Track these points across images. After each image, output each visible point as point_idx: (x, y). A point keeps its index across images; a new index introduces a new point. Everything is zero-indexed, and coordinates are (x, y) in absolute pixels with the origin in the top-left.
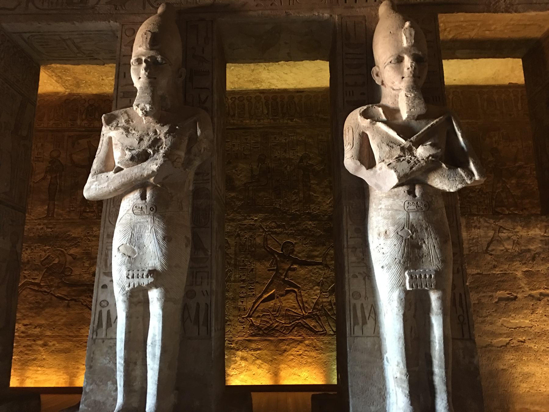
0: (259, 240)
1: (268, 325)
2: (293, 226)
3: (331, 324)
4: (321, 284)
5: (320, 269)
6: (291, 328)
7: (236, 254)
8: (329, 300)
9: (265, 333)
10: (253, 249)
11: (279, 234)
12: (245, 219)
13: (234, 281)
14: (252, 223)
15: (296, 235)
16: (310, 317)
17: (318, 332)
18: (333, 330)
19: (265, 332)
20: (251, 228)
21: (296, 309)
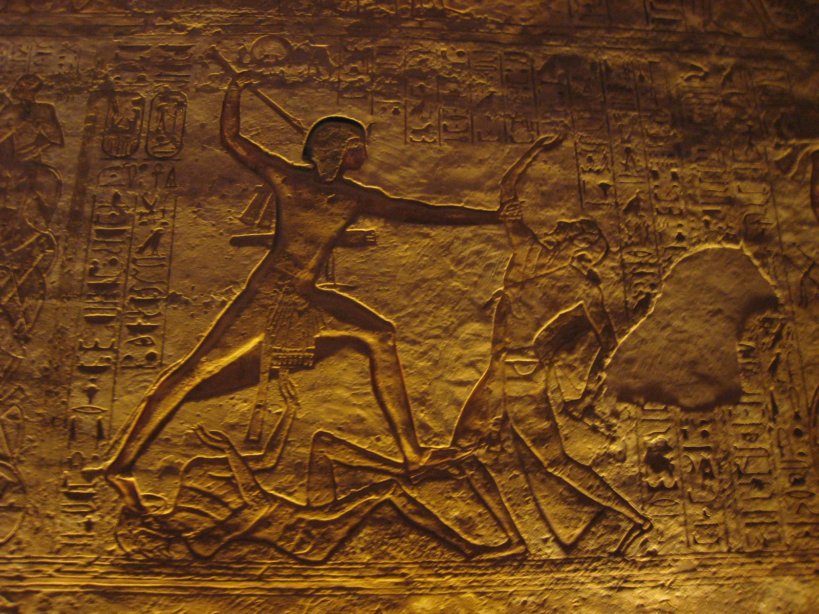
0: (200, 113)
1: (219, 515)
2: (366, 56)
3: (548, 511)
4: (498, 313)
5: (488, 240)
6: (340, 533)
7: (83, 170)
8: (538, 387)
9: (197, 557)
10: (170, 148)
11: (295, 85)
12: (144, 28)
13: (62, 293)
14: (174, 43)
15: (379, 94)
16: (444, 476)
17: (486, 549)
18: (557, 540)
19: (200, 549)
20: (169, 63)
21: (367, 434)
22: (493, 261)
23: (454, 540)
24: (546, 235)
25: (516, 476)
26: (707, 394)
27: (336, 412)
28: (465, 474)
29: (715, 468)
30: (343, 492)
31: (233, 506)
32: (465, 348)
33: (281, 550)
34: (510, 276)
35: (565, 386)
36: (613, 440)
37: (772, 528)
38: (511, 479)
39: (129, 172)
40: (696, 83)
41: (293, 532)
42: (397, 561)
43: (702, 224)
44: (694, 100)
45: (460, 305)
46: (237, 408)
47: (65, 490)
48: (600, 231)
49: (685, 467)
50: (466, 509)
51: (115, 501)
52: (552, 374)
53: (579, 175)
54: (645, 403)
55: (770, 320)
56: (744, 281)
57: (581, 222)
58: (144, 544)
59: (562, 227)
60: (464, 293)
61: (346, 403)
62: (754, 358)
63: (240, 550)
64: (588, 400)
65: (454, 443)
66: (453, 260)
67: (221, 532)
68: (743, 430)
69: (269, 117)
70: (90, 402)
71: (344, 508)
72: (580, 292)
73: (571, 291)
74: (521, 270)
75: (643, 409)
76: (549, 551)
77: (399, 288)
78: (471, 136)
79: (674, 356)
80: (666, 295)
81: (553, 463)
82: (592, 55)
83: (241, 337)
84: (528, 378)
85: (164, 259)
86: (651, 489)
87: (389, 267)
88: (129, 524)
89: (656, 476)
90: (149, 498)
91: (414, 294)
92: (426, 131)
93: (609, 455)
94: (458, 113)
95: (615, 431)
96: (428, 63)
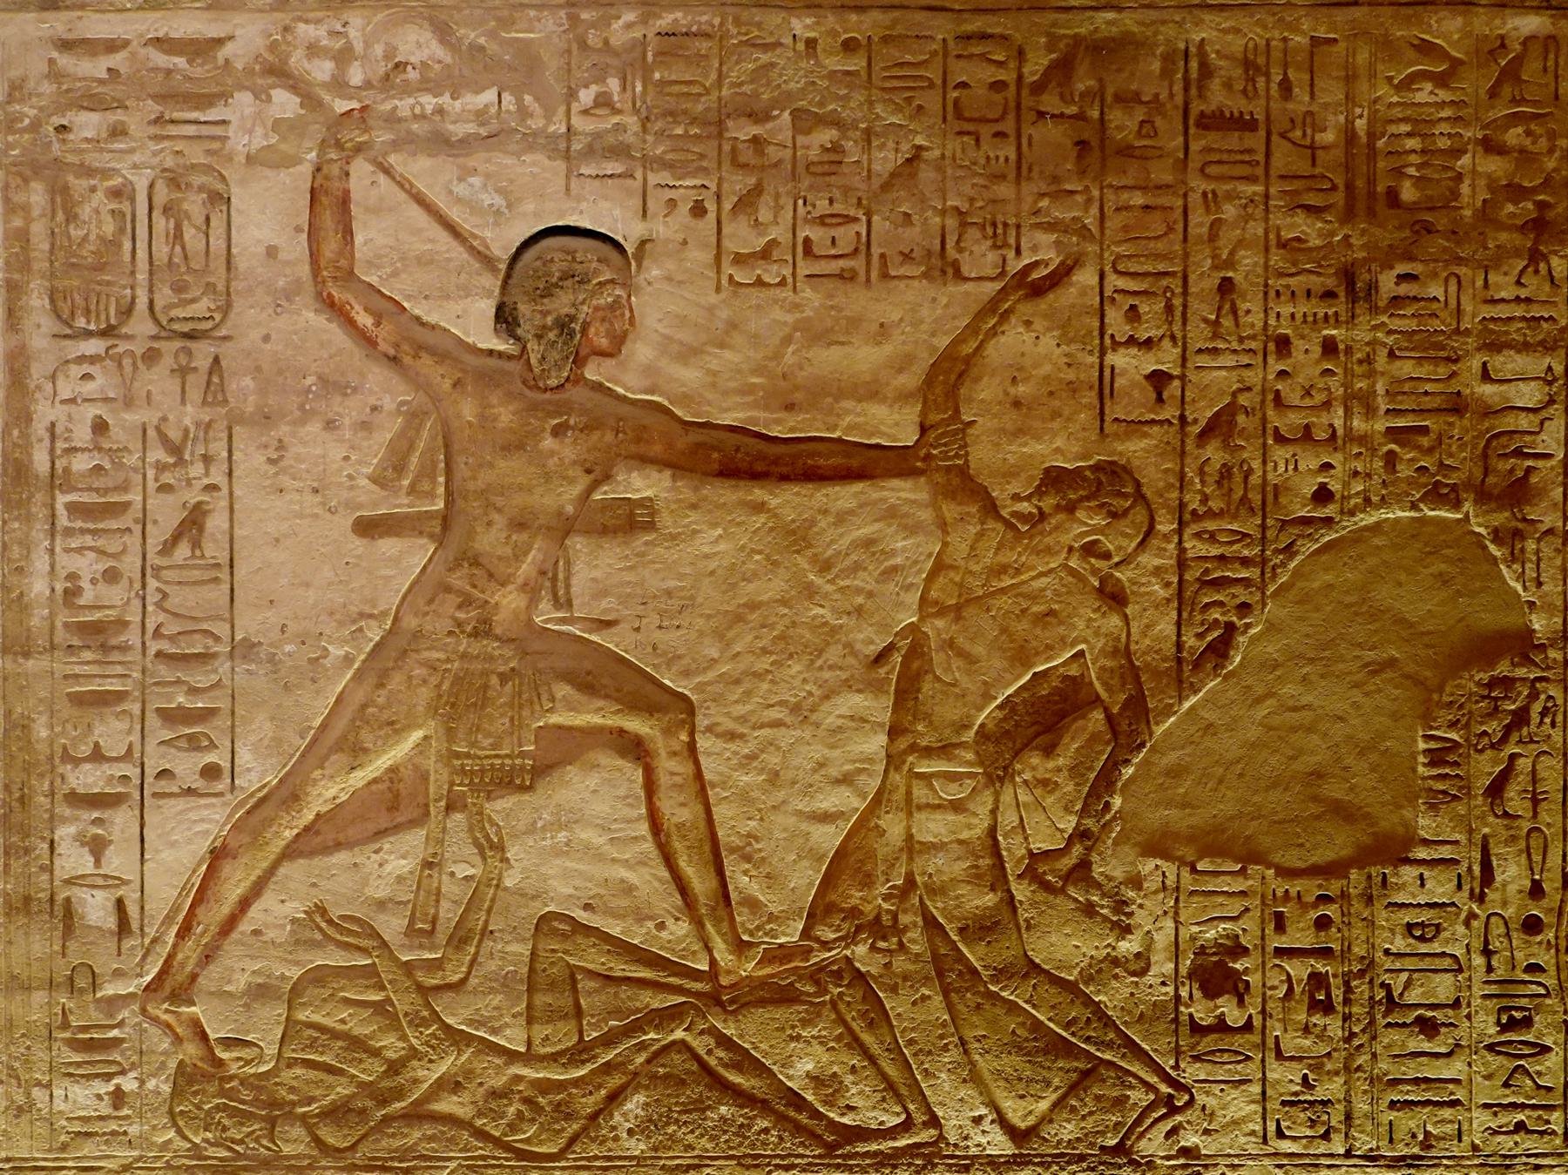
5: (891, 514)
6: (589, 1103)
10: (201, 307)
16: (784, 996)
17: (862, 1134)
18: (1002, 1121)
22: (898, 560)
23: (803, 1118)
24: (1016, 497)
25: (924, 998)
26: (1337, 843)
27: (581, 873)
28: (826, 992)
29: (1337, 994)
30: (595, 1026)
31: (391, 1055)
32: (832, 747)
33: (482, 1135)
34: (933, 594)
35: (1034, 820)
36: (1126, 930)
37: (1447, 1113)
38: (914, 1003)
39: (120, 365)
40: (1424, 93)
41: (505, 1101)
42: (696, 1153)
43: (1379, 464)
44: (1412, 143)
45: (825, 656)
46: (388, 868)
47: (67, 1035)
48: (1138, 485)
49: (1273, 988)
50: (825, 1058)
51: (165, 1053)
52: (1007, 796)
53: (1102, 354)
54: (1200, 858)
55: (1507, 683)
56: (1459, 593)
57: (1097, 468)
58: (225, 1129)
59: (1054, 479)
60: (834, 630)
61: (599, 857)
62: (1456, 764)
63: (406, 1136)
64: (1077, 850)
65: (806, 933)
66: (814, 560)
67: (369, 1104)
68: (1408, 917)
69: (417, 232)
70: (98, 863)
71: (595, 1057)
72: (1081, 624)
73: (1061, 623)
74: (957, 579)
75: (1194, 870)
76: (984, 1141)
77: (700, 622)
78: (865, 266)
79: (1273, 760)
80: (1271, 627)
81: (1002, 974)
82: (1169, 31)
83: (388, 730)
84: (957, 806)
85: (218, 565)
86: (1196, 1028)
87: (681, 577)
88: (195, 1093)
89: (1211, 1004)
90: (228, 1043)
91: (730, 634)
92: (765, 254)
93: (1115, 962)
94: (838, 208)
95: (1131, 914)
96: (773, 74)
